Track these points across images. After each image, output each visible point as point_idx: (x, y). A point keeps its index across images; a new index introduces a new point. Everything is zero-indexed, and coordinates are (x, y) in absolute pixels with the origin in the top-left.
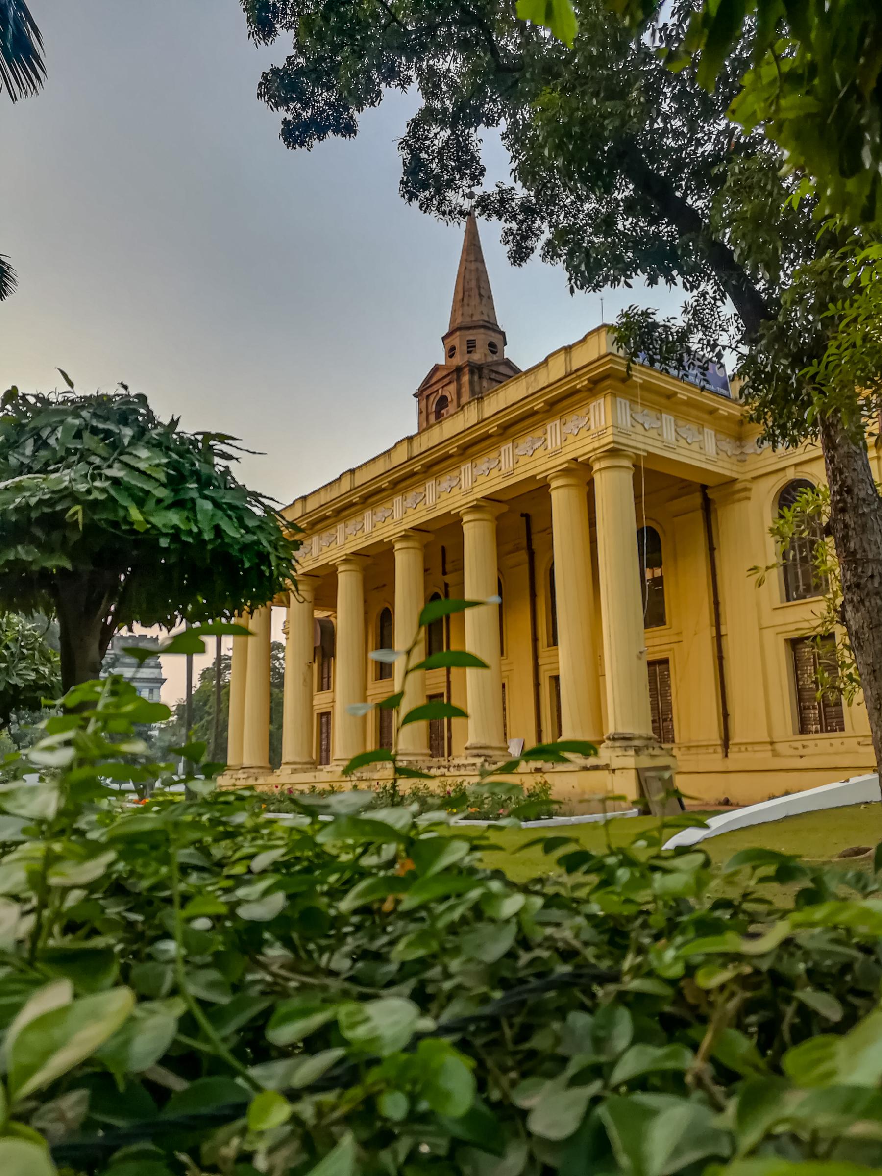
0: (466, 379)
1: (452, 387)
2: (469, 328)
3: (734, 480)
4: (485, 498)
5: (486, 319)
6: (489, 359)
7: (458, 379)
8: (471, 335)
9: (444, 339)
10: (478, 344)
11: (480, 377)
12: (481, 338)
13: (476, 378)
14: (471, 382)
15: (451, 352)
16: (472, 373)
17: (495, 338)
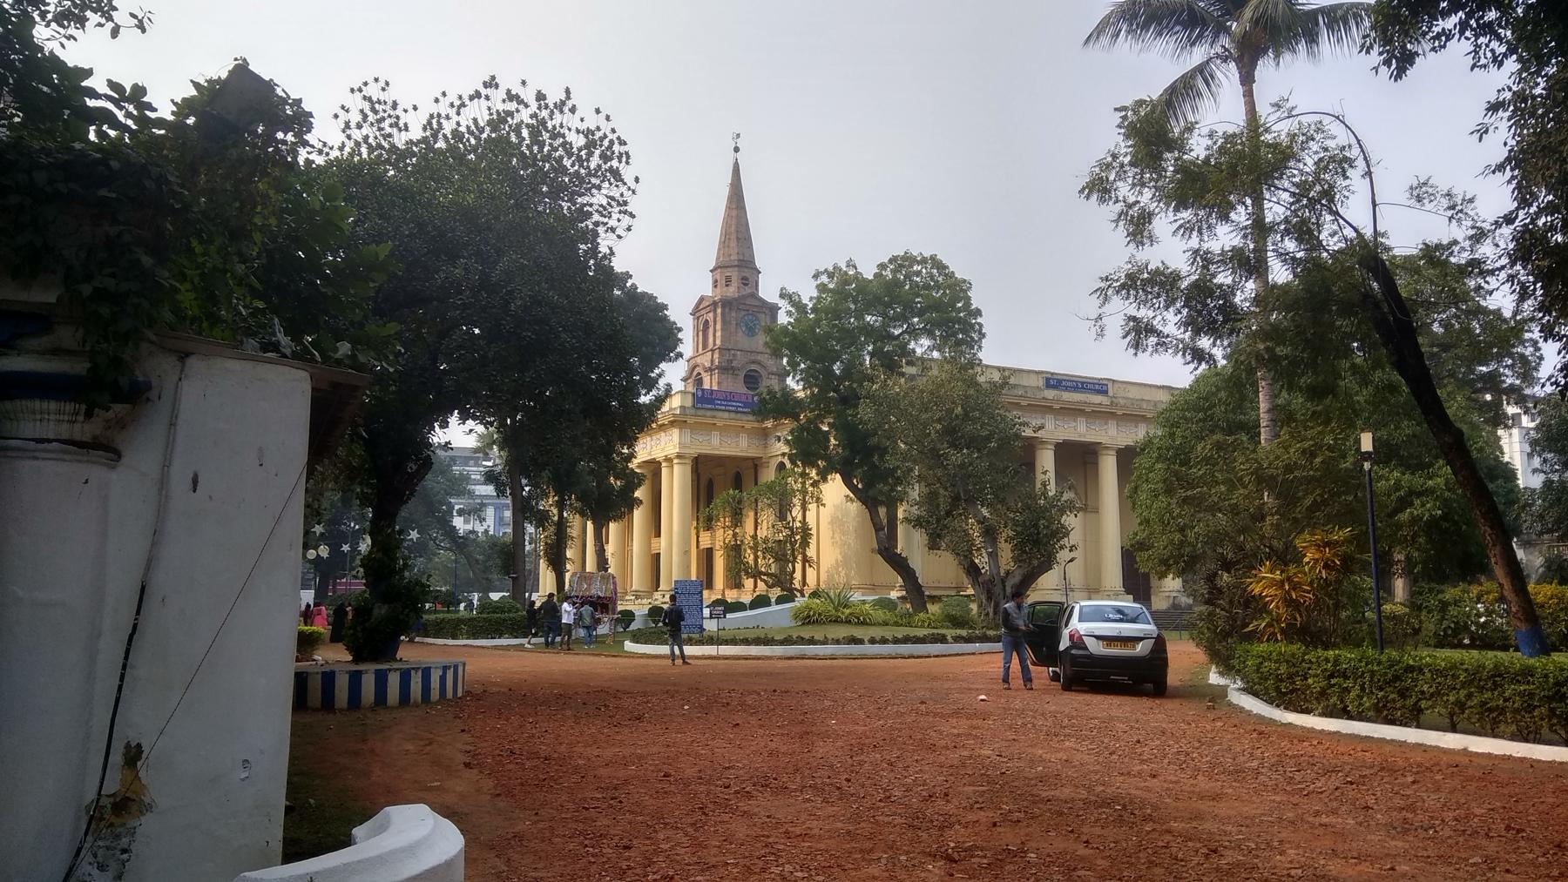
10: (734, 279)
16: (723, 307)
17: (747, 273)
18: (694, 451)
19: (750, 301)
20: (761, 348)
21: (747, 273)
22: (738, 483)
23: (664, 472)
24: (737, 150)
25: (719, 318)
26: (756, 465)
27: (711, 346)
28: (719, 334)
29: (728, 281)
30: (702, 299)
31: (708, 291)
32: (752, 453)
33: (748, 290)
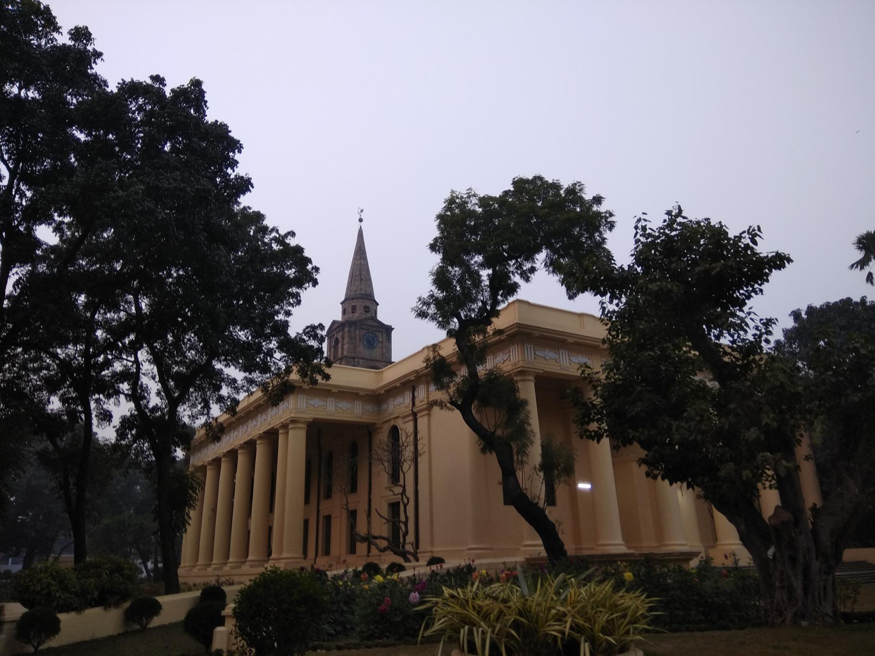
0: (346, 329)
1: (340, 334)
2: (353, 299)
3: (374, 424)
4: (264, 433)
5: (363, 292)
6: (364, 316)
7: (343, 329)
8: (354, 303)
9: (341, 303)
11: (356, 329)
12: (359, 304)
13: (352, 329)
14: (349, 332)
15: (344, 312)
16: (350, 326)
18: (310, 416)
19: (370, 323)
20: (379, 357)
21: (367, 303)
22: (354, 450)
23: (281, 437)
24: (361, 220)
25: (346, 335)
26: (368, 430)
27: (340, 355)
28: (346, 347)
29: (354, 309)
30: (334, 322)
31: (339, 317)
32: (366, 419)
33: (368, 315)
